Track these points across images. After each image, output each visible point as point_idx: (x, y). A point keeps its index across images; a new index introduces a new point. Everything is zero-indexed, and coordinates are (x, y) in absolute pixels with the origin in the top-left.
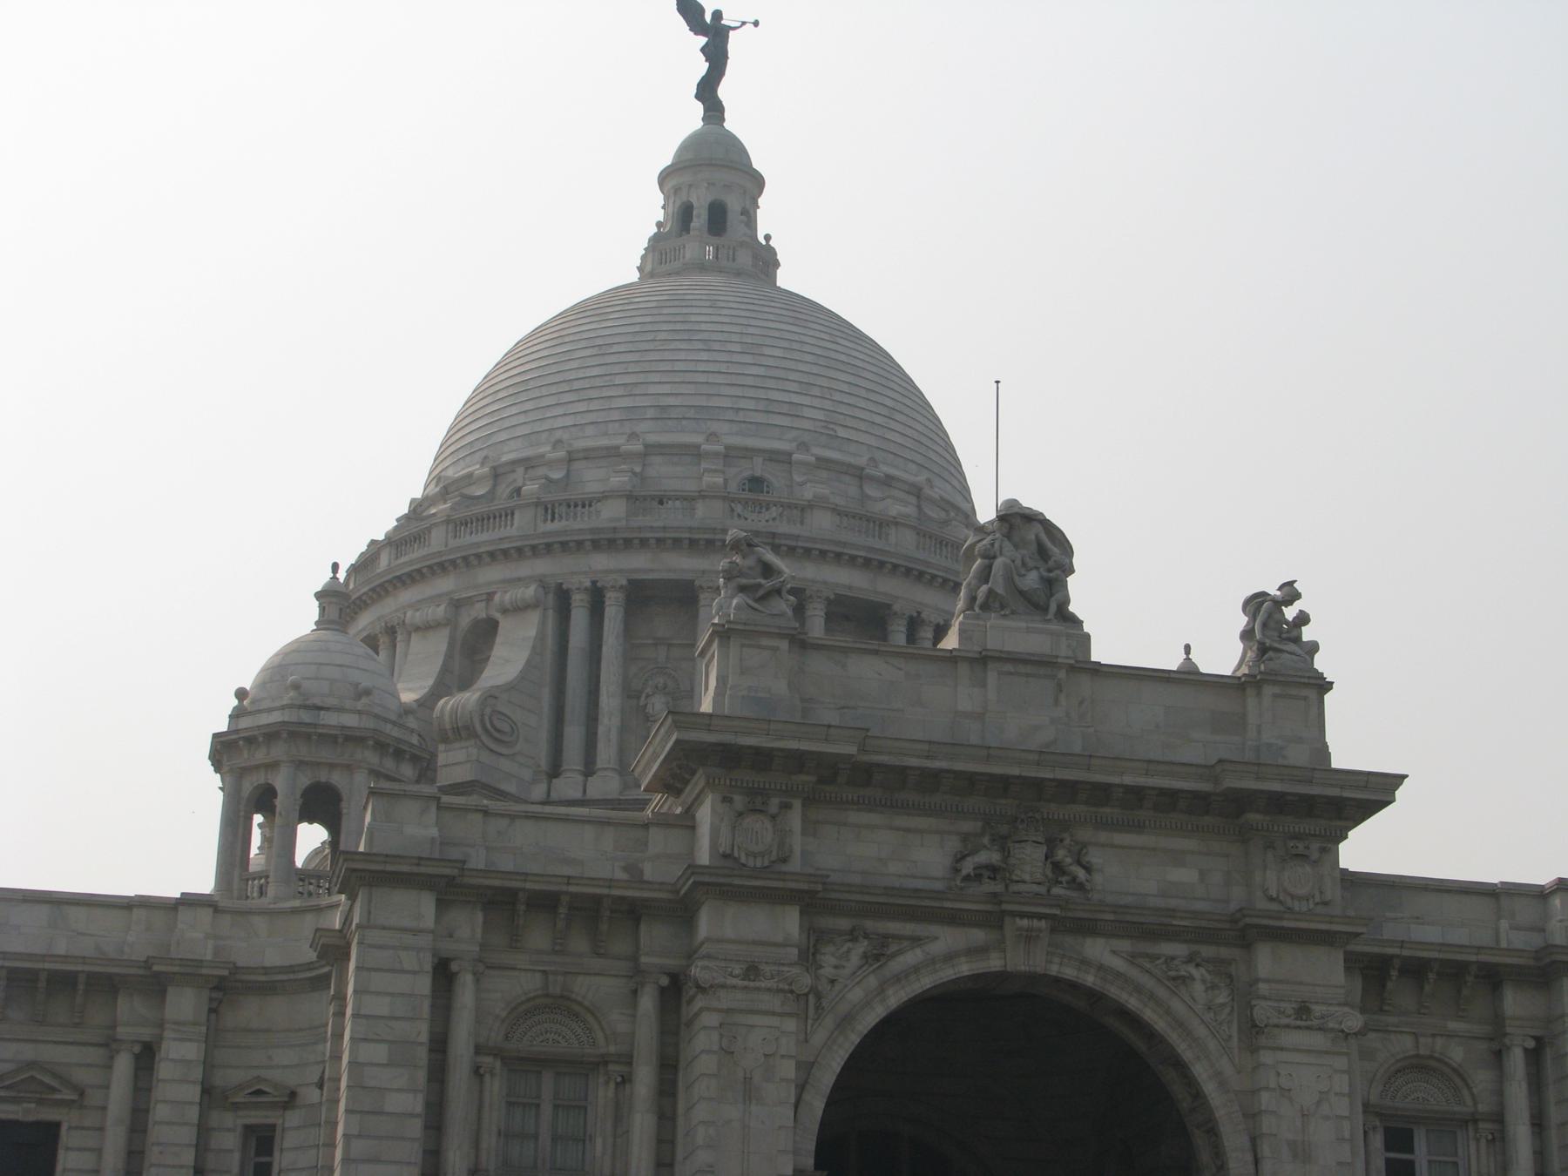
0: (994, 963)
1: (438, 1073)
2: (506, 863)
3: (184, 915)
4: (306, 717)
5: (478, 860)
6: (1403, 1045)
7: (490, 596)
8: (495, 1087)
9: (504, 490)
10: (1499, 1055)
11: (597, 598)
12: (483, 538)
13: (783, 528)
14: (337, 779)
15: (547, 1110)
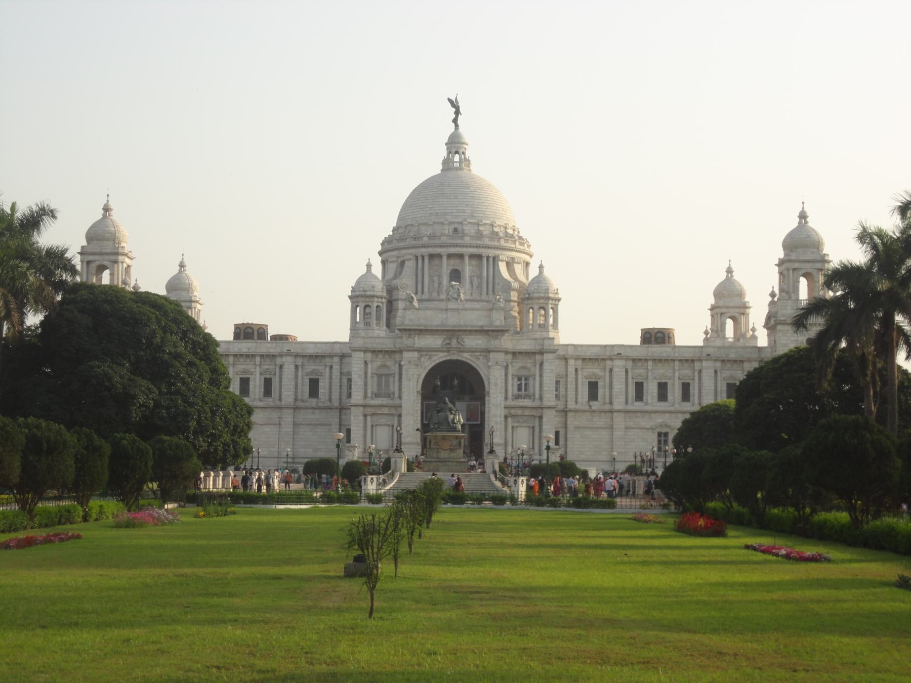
0: (448, 358)
1: (366, 377)
2: (375, 346)
3: (335, 345)
4: (364, 293)
5: (370, 346)
6: (520, 365)
7: (403, 256)
8: (376, 379)
9: (407, 231)
10: (535, 365)
11: (423, 257)
12: (402, 244)
13: (459, 241)
14: (370, 304)
15: (383, 381)
